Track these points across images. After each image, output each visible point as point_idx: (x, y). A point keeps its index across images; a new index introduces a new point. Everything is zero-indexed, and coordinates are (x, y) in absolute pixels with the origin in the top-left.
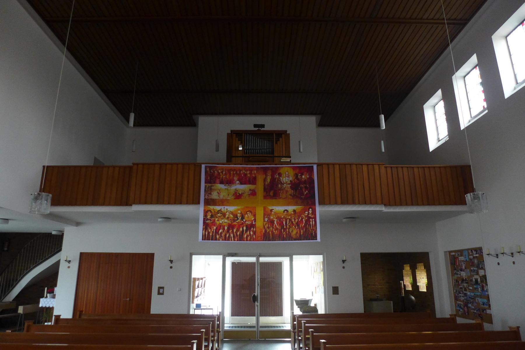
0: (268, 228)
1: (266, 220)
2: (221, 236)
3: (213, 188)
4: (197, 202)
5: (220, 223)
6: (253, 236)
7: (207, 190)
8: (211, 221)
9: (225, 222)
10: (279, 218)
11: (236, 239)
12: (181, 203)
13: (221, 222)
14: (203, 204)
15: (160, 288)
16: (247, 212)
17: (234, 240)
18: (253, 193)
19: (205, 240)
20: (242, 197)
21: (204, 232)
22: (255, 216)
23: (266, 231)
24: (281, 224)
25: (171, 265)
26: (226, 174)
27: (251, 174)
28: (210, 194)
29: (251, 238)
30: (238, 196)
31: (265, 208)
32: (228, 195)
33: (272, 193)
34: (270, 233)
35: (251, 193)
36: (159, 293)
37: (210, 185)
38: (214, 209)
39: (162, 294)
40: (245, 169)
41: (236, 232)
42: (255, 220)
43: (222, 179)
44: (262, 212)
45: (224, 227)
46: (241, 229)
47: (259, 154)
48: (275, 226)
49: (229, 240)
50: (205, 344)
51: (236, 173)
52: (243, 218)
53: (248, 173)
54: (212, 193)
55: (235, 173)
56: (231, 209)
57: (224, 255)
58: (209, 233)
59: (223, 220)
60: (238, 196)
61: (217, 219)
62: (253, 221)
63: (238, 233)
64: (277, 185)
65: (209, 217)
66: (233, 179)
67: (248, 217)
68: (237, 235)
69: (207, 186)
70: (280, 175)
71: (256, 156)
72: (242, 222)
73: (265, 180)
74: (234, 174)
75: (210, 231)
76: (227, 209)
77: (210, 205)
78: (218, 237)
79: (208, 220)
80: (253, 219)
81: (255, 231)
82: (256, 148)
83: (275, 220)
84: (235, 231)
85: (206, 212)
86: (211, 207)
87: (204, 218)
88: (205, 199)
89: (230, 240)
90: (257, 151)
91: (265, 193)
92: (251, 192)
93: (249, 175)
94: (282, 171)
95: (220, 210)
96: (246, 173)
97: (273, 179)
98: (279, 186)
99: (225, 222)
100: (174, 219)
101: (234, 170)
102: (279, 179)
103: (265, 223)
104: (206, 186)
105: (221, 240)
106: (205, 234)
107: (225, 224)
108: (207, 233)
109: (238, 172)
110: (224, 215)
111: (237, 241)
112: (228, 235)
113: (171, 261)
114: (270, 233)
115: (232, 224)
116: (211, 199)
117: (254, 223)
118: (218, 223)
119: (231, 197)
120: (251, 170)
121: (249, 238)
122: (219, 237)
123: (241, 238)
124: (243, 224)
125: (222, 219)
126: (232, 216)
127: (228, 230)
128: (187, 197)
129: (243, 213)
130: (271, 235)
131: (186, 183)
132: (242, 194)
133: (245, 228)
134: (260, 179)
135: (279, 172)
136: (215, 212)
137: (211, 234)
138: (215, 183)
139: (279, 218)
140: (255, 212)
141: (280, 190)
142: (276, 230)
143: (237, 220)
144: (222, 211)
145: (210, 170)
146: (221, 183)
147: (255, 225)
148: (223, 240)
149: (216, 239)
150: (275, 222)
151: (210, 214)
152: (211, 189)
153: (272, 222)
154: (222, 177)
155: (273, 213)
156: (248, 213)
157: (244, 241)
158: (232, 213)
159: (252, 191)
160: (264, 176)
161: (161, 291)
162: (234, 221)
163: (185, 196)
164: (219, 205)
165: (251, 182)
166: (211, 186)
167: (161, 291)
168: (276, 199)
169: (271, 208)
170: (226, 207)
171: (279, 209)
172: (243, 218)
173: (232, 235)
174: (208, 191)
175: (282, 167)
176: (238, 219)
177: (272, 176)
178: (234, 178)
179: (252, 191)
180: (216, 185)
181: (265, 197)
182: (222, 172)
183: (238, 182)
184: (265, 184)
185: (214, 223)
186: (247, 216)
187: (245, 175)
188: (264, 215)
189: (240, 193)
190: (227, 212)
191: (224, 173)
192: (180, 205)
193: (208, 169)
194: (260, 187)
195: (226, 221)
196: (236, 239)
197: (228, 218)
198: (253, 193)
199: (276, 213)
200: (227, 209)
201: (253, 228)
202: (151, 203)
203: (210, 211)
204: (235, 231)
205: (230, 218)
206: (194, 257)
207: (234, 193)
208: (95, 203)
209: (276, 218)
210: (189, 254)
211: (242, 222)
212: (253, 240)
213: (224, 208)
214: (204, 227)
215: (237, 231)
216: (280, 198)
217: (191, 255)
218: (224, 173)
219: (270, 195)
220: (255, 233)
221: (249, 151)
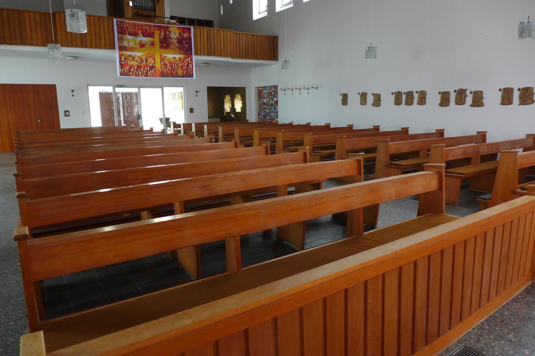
0: (164, 69)
1: (162, 63)
2: (133, 73)
3: (124, 38)
4: (113, 47)
5: (131, 64)
6: (154, 74)
7: (120, 39)
8: (125, 62)
9: (134, 63)
10: (170, 63)
11: (143, 76)
12: (100, 48)
13: (132, 64)
14: (118, 50)
15: (65, 112)
16: (149, 57)
17: (142, 76)
18: (153, 44)
19: (122, 76)
20: (145, 46)
21: (121, 70)
22: (154, 60)
23: (162, 71)
24: (171, 66)
25: (73, 94)
26: (132, 28)
27: (150, 29)
28: (122, 42)
29: (153, 75)
30: (142, 45)
31: (161, 55)
32: (135, 44)
33: (165, 45)
34: (165, 72)
35: (151, 44)
36: (66, 115)
37: (121, 35)
38: (126, 54)
39: (69, 116)
40: (145, 25)
41: (143, 71)
42: (155, 63)
43: (130, 32)
44: (159, 58)
45: (134, 67)
46: (146, 69)
47: (145, 10)
48: (168, 68)
49: (138, 76)
50: (181, 125)
51: (140, 28)
52: (147, 61)
53: (148, 29)
54: (124, 42)
55: (139, 28)
56: (139, 54)
57: (114, 87)
58: (124, 71)
59: (133, 62)
60: (142, 45)
61: (129, 61)
62: (154, 64)
63: (144, 72)
64: (168, 40)
65: (123, 59)
66: (138, 33)
67: (150, 61)
68: (143, 73)
69: (120, 37)
70: (170, 32)
71: (144, 12)
72: (147, 64)
73: (160, 35)
74: (138, 28)
75: (125, 69)
76: (135, 54)
77: (123, 51)
78: (131, 74)
79: (122, 61)
80: (153, 62)
81: (155, 71)
82: (142, 5)
83: (168, 64)
84: (142, 70)
85: (121, 56)
86: (124, 52)
87: (119, 60)
88: (119, 46)
89: (139, 76)
90: (146, 8)
91: (161, 44)
92: (151, 43)
93: (149, 31)
94: (171, 29)
95: (130, 55)
96: (147, 28)
97: (165, 35)
98: (170, 40)
99: (134, 63)
100: (80, 58)
101: (139, 25)
102: (169, 36)
103: (161, 65)
104: (118, 36)
105: (133, 76)
106: (122, 71)
107: (135, 65)
108: (123, 71)
109: (141, 28)
110: (134, 58)
111: (144, 77)
112: (137, 73)
113: (73, 91)
114: (165, 72)
115: (139, 65)
116: (123, 46)
117: (154, 65)
118: (130, 64)
119: (137, 46)
120: (150, 26)
121: (152, 75)
122: (132, 74)
123: (146, 75)
124: (147, 65)
125: (132, 61)
126: (139, 59)
127: (137, 70)
128: (105, 43)
129: (146, 57)
130: (166, 74)
131: (102, 33)
132: (145, 44)
133: (148, 68)
134: (157, 33)
135: (169, 30)
136: (127, 56)
137: (126, 72)
138: (125, 34)
139: (170, 63)
140: (155, 58)
141: (170, 43)
142: (168, 70)
143: (143, 62)
144: (132, 56)
145: (120, 24)
146: (130, 34)
147: (155, 66)
148: (134, 76)
149: (130, 75)
150: (168, 65)
151: (124, 57)
152: (122, 39)
153: (166, 65)
154: (130, 30)
155: (166, 59)
156: (150, 58)
157: (149, 77)
158: (139, 57)
159: (152, 42)
160: (159, 32)
161: (67, 113)
162: (141, 63)
163: (103, 42)
164: (130, 51)
165: (151, 36)
166: (122, 36)
167: (67, 113)
168: (168, 49)
169: (165, 55)
170: (135, 53)
171: (170, 56)
172: (147, 61)
173: (140, 73)
174: (121, 40)
175: (171, 27)
176: (144, 62)
177: (165, 32)
178: (139, 32)
179: (152, 42)
180: (126, 36)
181: (161, 47)
182: (129, 26)
183: (141, 35)
184: (160, 38)
185: (127, 64)
186: (149, 60)
187: (146, 30)
188: (161, 60)
189: (144, 43)
190: (135, 57)
191: (131, 27)
192: (100, 49)
193: (119, 23)
194: (157, 40)
195: (135, 63)
196: (143, 76)
197: (137, 61)
198: (153, 44)
199: (168, 59)
200: (135, 54)
201: (154, 69)
202: (77, 46)
203: (124, 55)
204: (142, 70)
205: (138, 61)
206: (89, 87)
207: (139, 43)
208: (23, 43)
209: (169, 63)
210: (86, 85)
211: (147, 64)
212: (155, 77)
213: (133, 54)
214: (120, 66)
215: (144, 70)
216: (171, 49)
217: (88, 85)
218: (131, 27)
219: (164, 47)
220: (155, 72)
221: (136, 7)
